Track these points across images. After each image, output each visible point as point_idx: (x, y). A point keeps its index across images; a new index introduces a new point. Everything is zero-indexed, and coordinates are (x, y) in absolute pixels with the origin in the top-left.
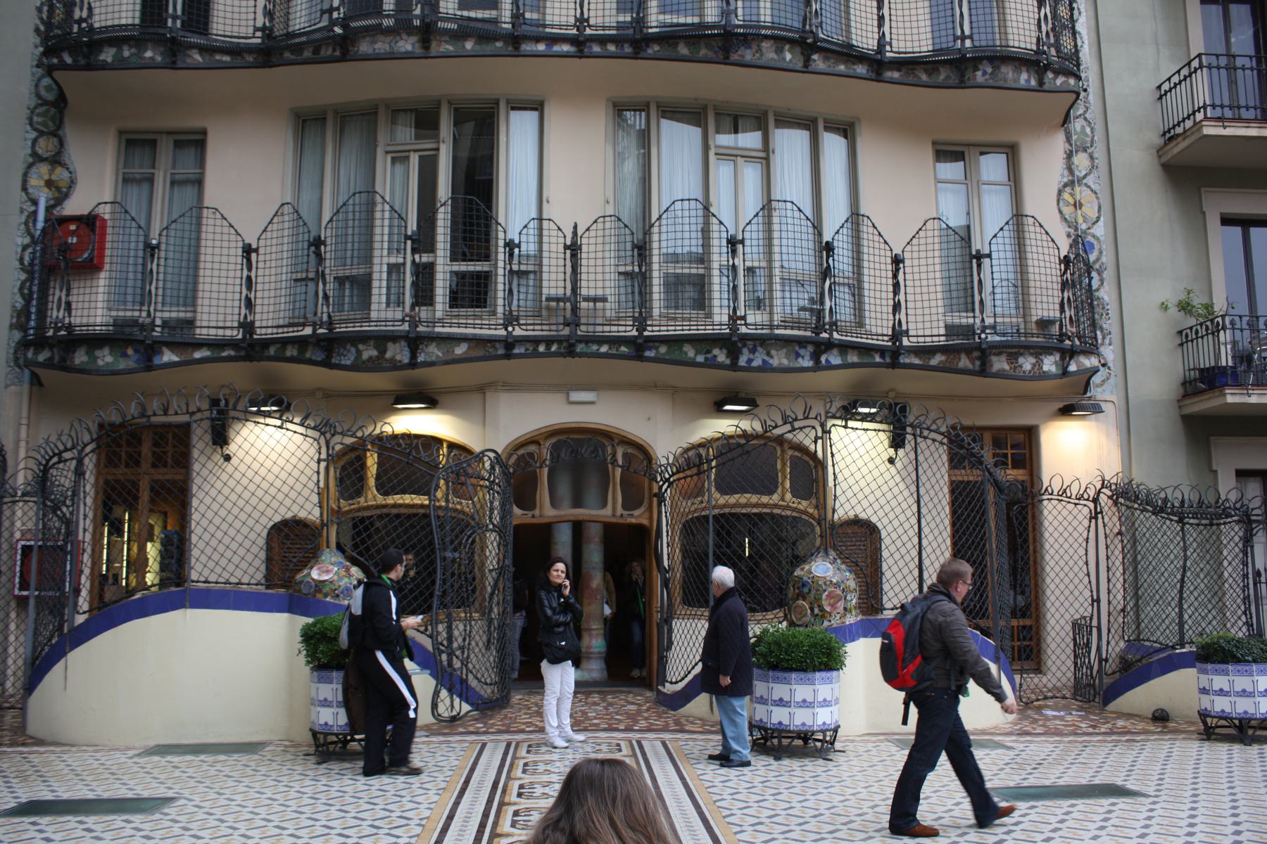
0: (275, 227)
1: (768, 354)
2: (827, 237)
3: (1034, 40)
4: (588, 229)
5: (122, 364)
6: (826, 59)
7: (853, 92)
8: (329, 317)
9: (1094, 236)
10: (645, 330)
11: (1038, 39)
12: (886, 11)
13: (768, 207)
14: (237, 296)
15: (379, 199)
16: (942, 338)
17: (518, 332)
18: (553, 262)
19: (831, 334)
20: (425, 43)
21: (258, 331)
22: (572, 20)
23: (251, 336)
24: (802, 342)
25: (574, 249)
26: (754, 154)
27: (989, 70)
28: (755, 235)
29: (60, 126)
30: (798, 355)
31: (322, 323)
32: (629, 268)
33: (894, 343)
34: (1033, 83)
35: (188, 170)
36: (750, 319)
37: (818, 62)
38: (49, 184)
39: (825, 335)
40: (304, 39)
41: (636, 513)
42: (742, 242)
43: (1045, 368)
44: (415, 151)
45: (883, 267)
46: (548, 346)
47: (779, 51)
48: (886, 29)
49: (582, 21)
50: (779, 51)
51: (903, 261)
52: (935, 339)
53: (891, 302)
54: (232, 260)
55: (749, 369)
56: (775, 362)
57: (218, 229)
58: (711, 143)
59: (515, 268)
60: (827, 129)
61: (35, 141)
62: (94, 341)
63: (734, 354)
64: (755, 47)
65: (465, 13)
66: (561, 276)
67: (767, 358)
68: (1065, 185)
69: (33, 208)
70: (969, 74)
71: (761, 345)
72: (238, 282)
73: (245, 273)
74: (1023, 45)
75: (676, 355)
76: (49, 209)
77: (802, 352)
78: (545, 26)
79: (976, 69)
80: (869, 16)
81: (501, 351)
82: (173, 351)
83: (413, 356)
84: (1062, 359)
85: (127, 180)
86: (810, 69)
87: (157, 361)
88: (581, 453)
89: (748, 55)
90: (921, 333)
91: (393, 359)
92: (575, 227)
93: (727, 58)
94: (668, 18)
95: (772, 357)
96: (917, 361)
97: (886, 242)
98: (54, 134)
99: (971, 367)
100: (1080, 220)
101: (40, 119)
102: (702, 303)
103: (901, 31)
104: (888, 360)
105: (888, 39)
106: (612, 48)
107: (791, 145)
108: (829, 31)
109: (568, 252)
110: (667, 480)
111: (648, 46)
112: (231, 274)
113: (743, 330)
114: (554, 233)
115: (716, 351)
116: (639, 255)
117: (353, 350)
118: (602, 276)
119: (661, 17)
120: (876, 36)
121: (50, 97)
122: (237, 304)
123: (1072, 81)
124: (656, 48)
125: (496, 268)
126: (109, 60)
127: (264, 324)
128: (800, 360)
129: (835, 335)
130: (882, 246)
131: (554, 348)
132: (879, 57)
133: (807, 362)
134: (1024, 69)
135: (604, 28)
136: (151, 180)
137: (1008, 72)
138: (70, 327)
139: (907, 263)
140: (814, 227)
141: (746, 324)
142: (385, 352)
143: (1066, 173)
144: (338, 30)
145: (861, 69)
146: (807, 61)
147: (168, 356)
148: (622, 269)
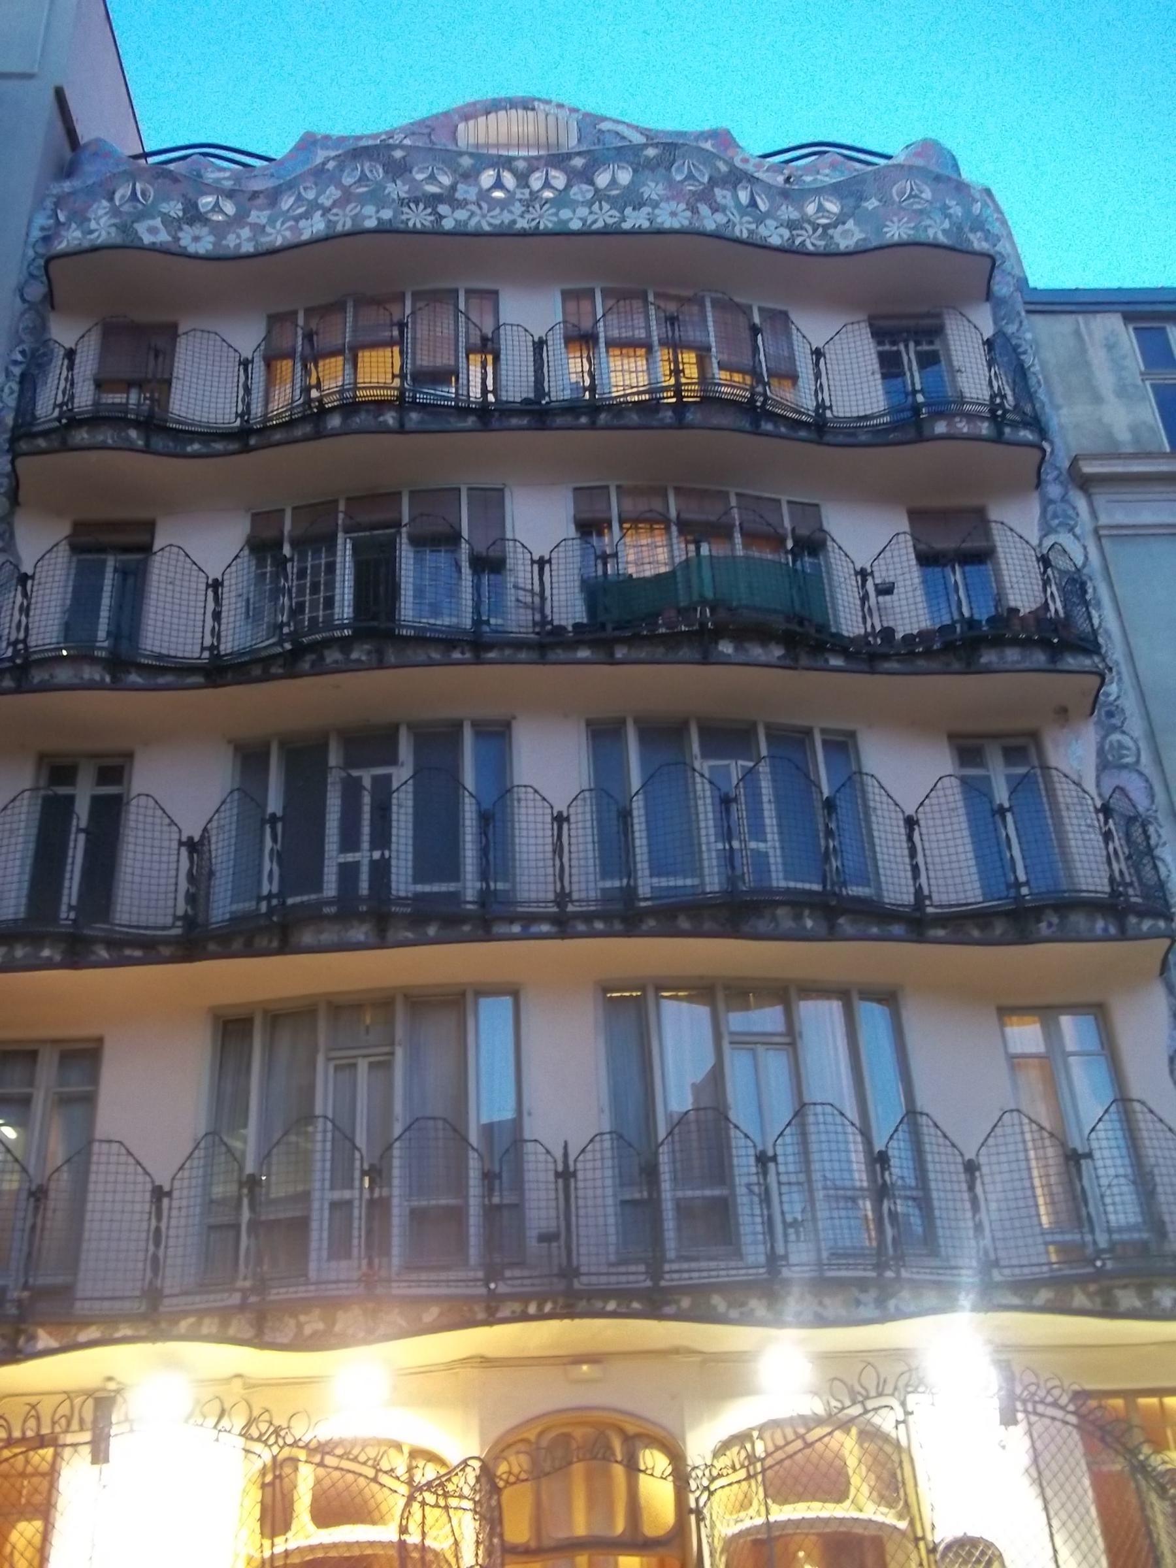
1: (820, 1303)
2: (879, 1146)
3: (1106, 881)
4: (583, 1151)
10: (662, 1278)
11: (1112, 880)
12: (920, 859)
13: (801, 1110)
14: (141, 1256)
17: (503, 1288)
22: (551, 896)
25: (566, 1175)
27: (1055, 920)
28: (790, 1150)
30: (858, 1303)
35: (76, 1088)
42: (774, 1158)
46: (540, 1307)
47: (798, 917)
48: (923, 880)
49: (562, 898)
50: (798, 917)
51: (978, 1168)
54: (138, 1207)
58: (723, 1029)
59: (496, 1200)
60: (862, 999)
72: (144, 1235)
73: (154, 1222)
74: (1092, 888)
77: (863, 1297)
79: (1039, 921)
80: (901, 867)
82: (50, 1334)
92: (566, 1147)
94: (664, 882)
95: (825, 1307)
97: (953, 1145)
105: (926, 892)
110: (707, 1488)
111: (641, 921)
114: (542, 1158)
117: (292, 1323)
120: (912, 890)
123: (1162, 924)
128: (862, 1309)
130: (950, 1150)
132: (918, 915)
140: (862, 1133)
142: (334, 1324)
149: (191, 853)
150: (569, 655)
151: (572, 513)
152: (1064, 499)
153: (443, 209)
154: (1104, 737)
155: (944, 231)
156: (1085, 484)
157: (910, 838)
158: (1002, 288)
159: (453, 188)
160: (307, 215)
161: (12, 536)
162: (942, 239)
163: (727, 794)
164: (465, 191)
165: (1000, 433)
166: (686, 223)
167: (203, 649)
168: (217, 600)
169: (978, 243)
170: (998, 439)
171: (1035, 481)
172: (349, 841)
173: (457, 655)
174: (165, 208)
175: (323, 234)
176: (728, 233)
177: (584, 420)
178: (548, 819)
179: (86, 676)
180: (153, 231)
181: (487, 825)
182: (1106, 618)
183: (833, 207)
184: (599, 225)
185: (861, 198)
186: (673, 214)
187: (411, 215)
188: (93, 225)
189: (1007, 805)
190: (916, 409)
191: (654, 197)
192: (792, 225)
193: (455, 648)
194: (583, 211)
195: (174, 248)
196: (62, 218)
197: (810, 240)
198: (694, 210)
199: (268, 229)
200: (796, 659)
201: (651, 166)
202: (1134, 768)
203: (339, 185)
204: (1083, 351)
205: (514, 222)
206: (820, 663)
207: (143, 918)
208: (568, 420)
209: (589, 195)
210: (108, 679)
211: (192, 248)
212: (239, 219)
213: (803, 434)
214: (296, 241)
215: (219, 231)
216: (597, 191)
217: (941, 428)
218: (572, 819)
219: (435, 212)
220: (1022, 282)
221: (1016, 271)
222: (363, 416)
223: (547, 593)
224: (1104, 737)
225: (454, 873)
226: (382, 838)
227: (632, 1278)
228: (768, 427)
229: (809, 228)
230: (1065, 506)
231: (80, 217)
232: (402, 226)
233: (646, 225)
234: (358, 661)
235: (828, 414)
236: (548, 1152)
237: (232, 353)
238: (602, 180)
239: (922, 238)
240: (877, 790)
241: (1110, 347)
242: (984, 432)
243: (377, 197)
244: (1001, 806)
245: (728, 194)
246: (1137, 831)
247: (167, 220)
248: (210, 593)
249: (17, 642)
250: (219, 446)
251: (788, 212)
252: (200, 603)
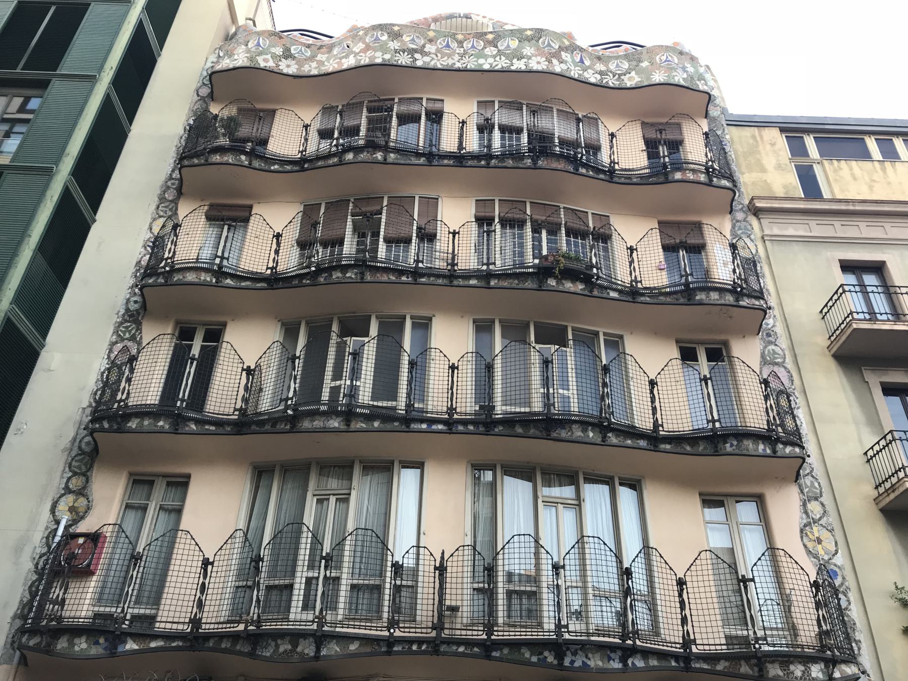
0: (229, 546)
2: (626, 565)
3: (765, 422)
4: (452, 555)
5: (95, 651)
6: (617, 436)
7: (640, 458)
8: (259, 616)
9: (835, 565)
10: (492, 634)
11: (768, 421)
12: (657, 404)
13: (581, 541)
14: (192, 598)
15: (305, 529)
16: (724, 647)
17: (398, 633)
18: (426, 579)
19: (634, 642)
20: (348, 422)
21: (203, 626)
22: (445, 409)
23: (197, 630)
24: (612, 647)
25: (441, 569)
26: (570, 502)
27: (735, 443)
28: (573, 562)
29: (90, 468)
30: (610, 659)
31: (252, 621)
32: (481, 585)
33: (685, 650)
34: (768, 451)
36: (571, 628)
37: (613, 439)
38: (72, 509)
39: (629, 642)
40: (266, 417)
42: (563, 567)
43: (814, 675)
44: (334, 495)
45: (670, 588)
47: (585, 431)
48: (658, 416)
49: (451, 410)
50: (585, 431)
51: (685, 583)
52: (719, 647)
53: (679, 616)
55: (571, 669)
56: (591, 663)
57: (187, 547)
58: (539, 494)
59: (398, 583)
60: (621, 484)
61: (69, 479)
62: (76, 631)
63: (560, 657)
64: (567, 426)
65: (375, 403)
66: (431, 591)
67: (585, 660)
68: (805, 526)
69: (55, 526)
70: (720, 445)
71: (581, 649)
72: (195, 586)
73: (201, 580)
74: (757, 426)
76: (66, 528)
77: (613, 655)
78: (427, 412)
80: (646, 407)
81: (384, 649)
82: (134, 642)
83: (318, 650)
84: (826, 667)
85: (128, 507)
86: (607, 443)
87: (120, 649)
89: (564, 434)
90: (705, 642)
91: (302, 654)
92: (443, 553)
93: (549, 435)
94: (508, 409)
96: (706, 667)
97: (671, 568)
98: (84, 474)
99: (751, 672)
100: (821, 552)
101: (77, 464)
102: (534, 614)
103: (669, 417)
104: (682, 665)
105: (660, 422)
106: (471, 427)
107: (595, 496)
108: (619, 418)
109: (437, 572)
112: (191, 580)
113: (567, 636)
114: (428, 557)
115: (546, 653)
116: (489, 575)
117: (273, 644)
118: (461, 591)
119: (504, 408)
120: (652, 421)
121: (87, 449)
122: (191, 604)
123: (797, 450)
124: (501, 428)
125: (385, 582)
126: (134, 426)
127: (209, 621)
128: (611, 662)
129: (638, 642)
130: (669, 571)
131: (424, 647)
133: (616, 665)
134: (760, 442)
135: (466, 414)
136: (144, 509)
137: (749, 444)
138: (60, 619)
139: (689, 584)
141: (568, 632)
143: (804, 516)
144: (290, 412)
145: (642, 443)
146: (604, 438)
147: (131, 645)
148: (476, 586)
149: (248, 375)
150: (466, 283)
151: (473, 211)
152: (745, 220)
153: (417, 56)
154: (765, 347)
155: (684, 79)
156: (757, 212)
157: (652, 392)
158: (714, 112)
159: (424, 46)
160: (347, 57)
161: (177, 209)
162: (682, 83)
163: (547, 358)
164: (429, 48)
165: (711, 181)
166: (545, 67)
167: (268, 268)
168: (278, 244)
169: (702, 87)
170: (710, 184)
171: (729, 210)
172: (337, 375)
173: (404, 278)
174: (273, 50)
175: (353, 66)
176: (567, 75)
177: (483, 163)
178: (447, 367)
179: (202, 278)
180: (266, 60)
181: (412, 368)
182: (768, 283)
183: (626, 65)
184: (499, 67)
185: (640, 61)
186: (539, 63)
187: (401, 58)
188: (236, 57)
189: (708, 376)
190: (665, 166)
191: (529, 54)
192: (601, 73)
193: (403, 275)
194: (491, 60)
195: (276, 70)
196: (221, 54)
197: (612, 81)
198: (550, 62)
199: (326, 63)
200: (591, 291)
201: (529, 39)
202: (782, 365)
203: (364, 42)
204: (757, 146)
205: (454, 64)
206: (605, 295)
207: (222, 409)
208: (475, 163)
209: (495, 53)
210: (214, 281)
211: (285, 71)
212: (312, 58)
213: (602, 176)
214: (340, 69)
215: (300, 63)
216: (499, 51)
217: (678, 176)
218: (460, 368)
219: (413, 57)
220: (724, 111)
221: (722, 104)
222: (365, 154)
223: (456, 252)
224: (765, 347)
225: (394, 398)
226: (355, 373)
227: (475, 633)
228: (583, 171)
229: (611, 75)
230: (745, 223)
231: (230, 54)
232: (395, 63)
233: (523, 68)
234: (350, 277)
235: (617, 167)
236: (431, 554)
237: (300, 121)
238: (502, 45)
239: (672, 82)
240: (634, 364)
241: (773, 145)
242: (702, 179)
243: (384, 49)
244: (705, 376)
245: (569, 56)
246: (783, 402)
247: (274, 56)
248: (275, 240)
249: (168, 258)
250: (288, 168)
251: (600, 67)
252: (269, 244)
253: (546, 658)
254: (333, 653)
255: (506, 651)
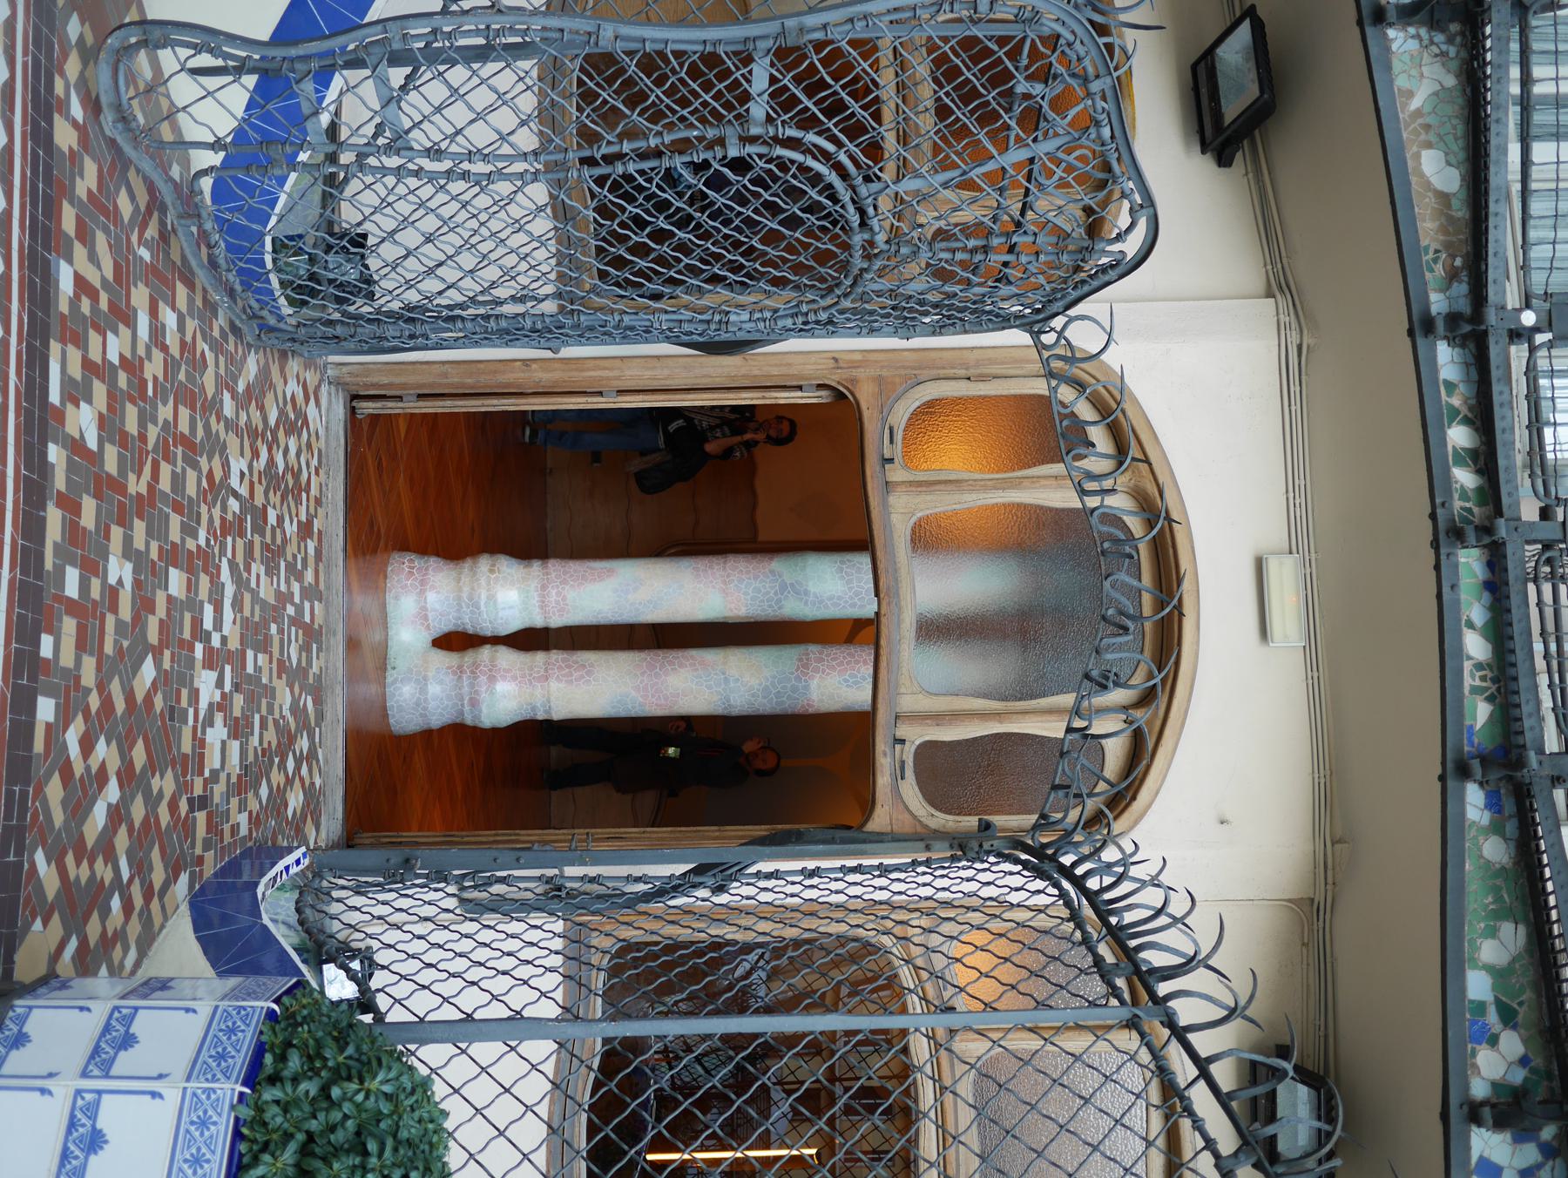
41: (910, 790)
75: (1477, 897)
88: (1109, 593)
115: (1512, 1044)
131: (1465, 478)
253: (1493, 1041)
254: (1401, 82)
255: (1495, 850)
